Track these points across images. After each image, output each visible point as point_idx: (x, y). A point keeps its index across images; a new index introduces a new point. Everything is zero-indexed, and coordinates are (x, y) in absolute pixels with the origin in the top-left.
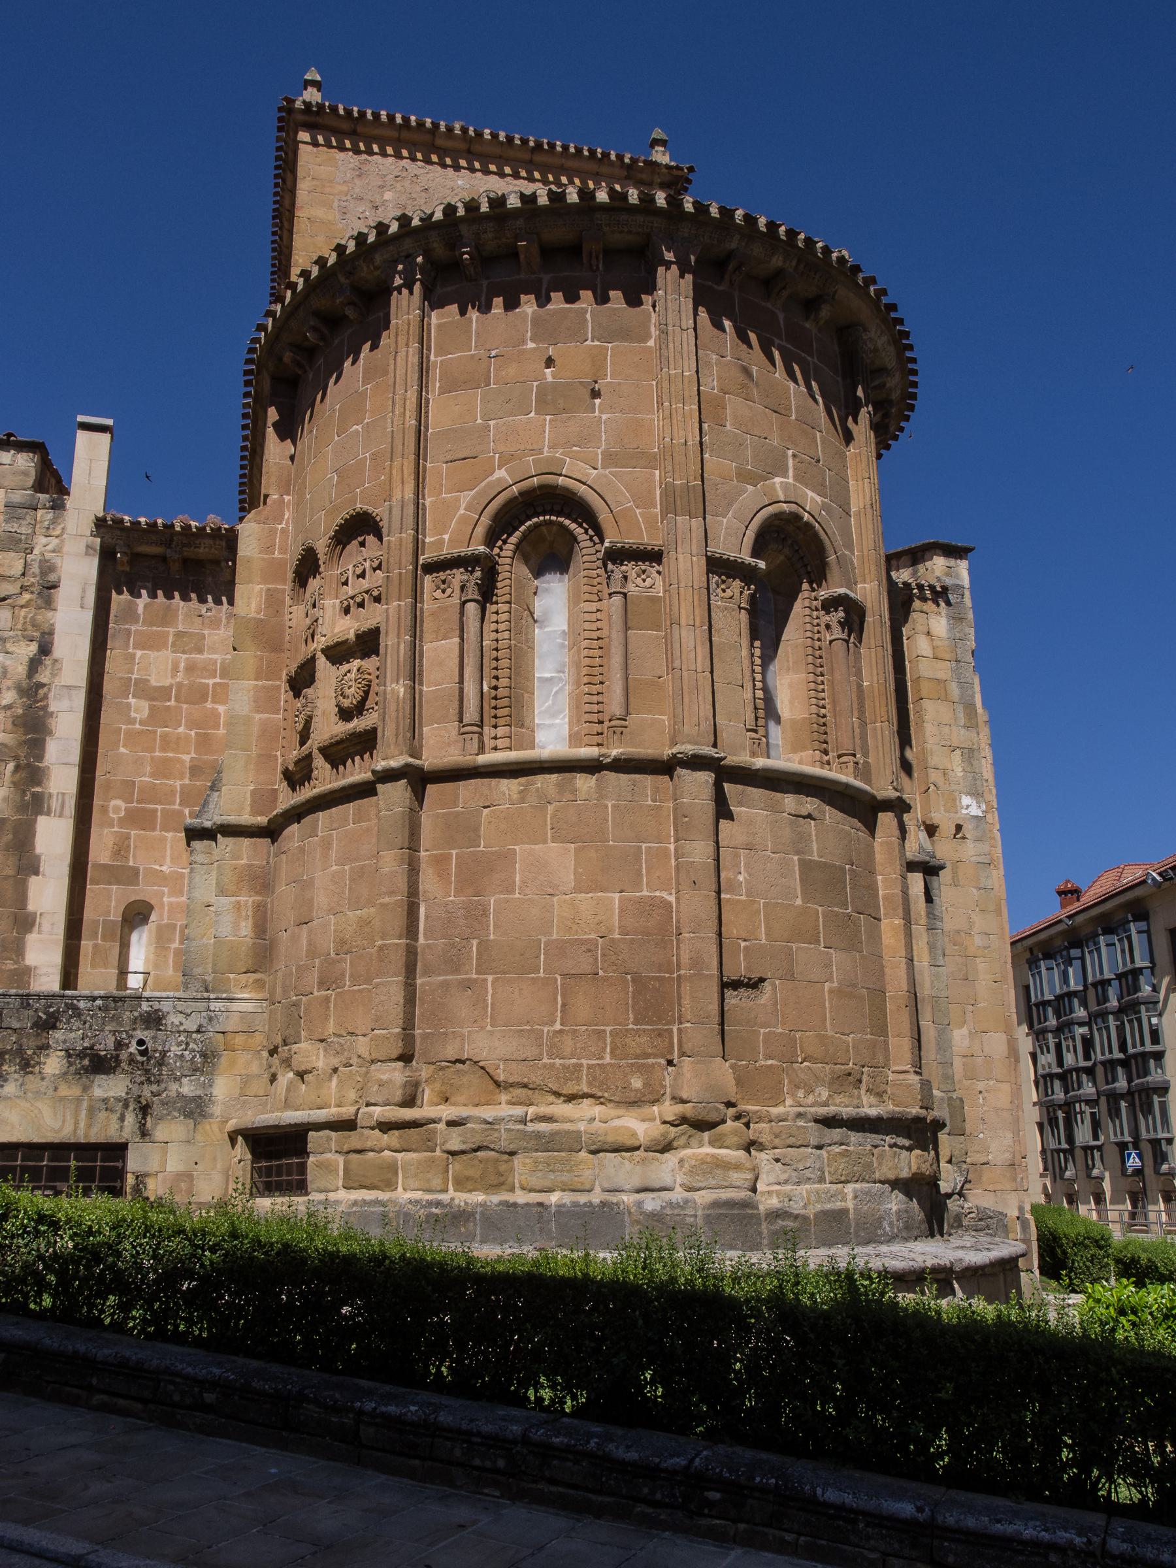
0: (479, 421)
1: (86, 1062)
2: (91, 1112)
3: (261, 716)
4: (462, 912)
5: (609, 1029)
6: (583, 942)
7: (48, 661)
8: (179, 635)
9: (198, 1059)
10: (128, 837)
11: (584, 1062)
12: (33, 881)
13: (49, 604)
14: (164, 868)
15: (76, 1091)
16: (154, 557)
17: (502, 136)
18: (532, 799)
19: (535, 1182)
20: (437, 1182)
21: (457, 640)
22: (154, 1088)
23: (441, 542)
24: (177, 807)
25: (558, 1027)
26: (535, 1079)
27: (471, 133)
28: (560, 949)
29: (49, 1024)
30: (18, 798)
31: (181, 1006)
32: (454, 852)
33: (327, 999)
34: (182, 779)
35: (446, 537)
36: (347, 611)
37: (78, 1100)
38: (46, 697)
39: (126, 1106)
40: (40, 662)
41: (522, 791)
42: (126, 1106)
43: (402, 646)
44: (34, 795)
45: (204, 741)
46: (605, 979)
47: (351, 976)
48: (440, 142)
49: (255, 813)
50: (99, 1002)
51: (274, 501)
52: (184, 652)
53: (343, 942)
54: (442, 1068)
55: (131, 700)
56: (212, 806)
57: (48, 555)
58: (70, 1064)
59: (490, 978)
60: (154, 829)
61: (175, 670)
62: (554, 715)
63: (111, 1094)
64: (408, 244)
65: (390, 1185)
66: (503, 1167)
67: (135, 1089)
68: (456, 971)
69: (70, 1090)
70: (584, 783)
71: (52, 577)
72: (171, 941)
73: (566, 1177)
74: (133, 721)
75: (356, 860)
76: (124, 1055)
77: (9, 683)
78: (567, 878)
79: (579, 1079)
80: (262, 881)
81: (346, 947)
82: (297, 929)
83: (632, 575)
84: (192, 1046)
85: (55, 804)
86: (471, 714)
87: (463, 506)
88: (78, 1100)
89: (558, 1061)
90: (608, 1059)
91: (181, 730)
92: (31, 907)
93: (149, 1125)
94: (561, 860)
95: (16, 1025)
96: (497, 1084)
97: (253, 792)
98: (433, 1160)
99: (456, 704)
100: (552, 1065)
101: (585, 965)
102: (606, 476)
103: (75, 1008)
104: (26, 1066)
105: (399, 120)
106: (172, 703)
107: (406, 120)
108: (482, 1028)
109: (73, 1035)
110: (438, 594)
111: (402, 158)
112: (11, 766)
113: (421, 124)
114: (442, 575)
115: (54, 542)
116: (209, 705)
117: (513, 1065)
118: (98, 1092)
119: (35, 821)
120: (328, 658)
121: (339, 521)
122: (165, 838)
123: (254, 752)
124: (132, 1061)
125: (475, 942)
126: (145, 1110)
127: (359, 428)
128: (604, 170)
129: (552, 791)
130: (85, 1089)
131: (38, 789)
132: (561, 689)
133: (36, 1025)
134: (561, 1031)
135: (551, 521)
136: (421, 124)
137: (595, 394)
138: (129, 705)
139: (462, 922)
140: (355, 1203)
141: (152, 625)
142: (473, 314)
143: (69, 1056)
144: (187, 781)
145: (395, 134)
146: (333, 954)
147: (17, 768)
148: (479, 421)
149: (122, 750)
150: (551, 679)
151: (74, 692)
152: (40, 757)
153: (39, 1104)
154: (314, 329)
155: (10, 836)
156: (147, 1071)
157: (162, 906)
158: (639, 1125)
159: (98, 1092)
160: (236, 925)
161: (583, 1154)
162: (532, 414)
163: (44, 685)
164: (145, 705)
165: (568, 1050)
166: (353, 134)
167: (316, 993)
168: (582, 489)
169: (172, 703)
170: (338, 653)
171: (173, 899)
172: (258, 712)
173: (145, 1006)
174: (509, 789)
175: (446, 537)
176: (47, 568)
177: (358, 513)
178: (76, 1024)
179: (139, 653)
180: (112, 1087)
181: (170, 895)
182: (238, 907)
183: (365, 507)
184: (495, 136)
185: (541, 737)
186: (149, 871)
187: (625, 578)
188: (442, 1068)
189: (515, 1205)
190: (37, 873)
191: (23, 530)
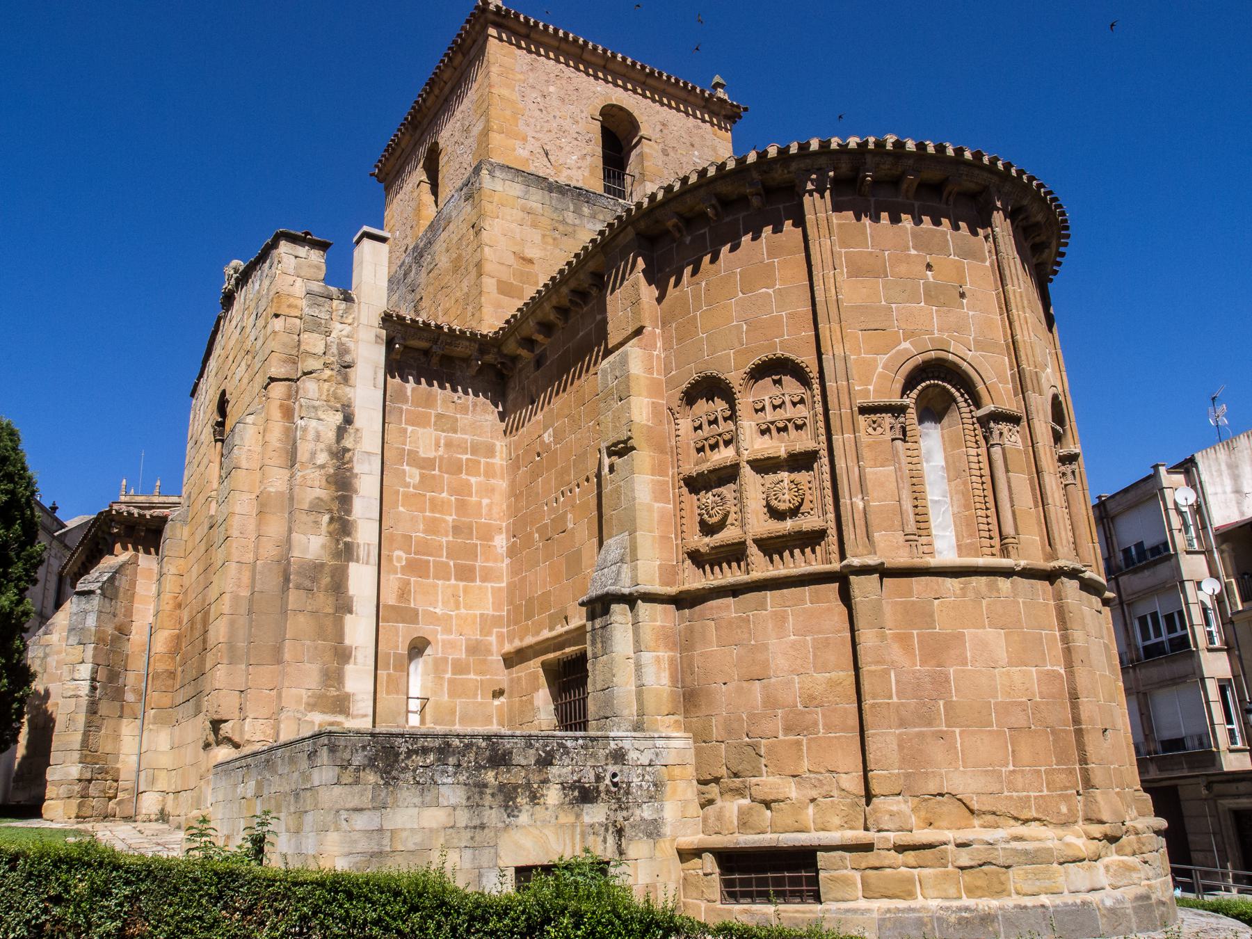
1: (576, 793)
2: (583, 835)
4: (927, 679)
5: (1043, 769)
6: (1021, 703)
7: (351, 429)
8: (439, 416)
9: (652, 789)
10: (408, 583)
11: (1032, 794)
12: (348, 618)
13: (346, 380)
14: (437, 610)
15: (571, 819)
16: (417, 350)
17: (629, 61)
18: (971, 595)
19: (1027, 888)
20: (952, 892)
22: (625, 813)
23: (868, 391)
24: (444, 559)
25: (1011, 768)
26: (1001, 808)
27: (609, 54)
28: (1005, 708)
29: (546, 761)
30: (333, 546)
31: (637, 744)
32: (915, 632)
33: (799, 743)
34: (447, 536)
35: (871, 388)
36: (763, 432)
37: (573, 826)
38: (351, 461)
39: (607, 830)
40: (345, 430)
42: (607, 830)
44: (346, 544)
45: (462, 506)
46: (1036, 731)
47: (825, 725)
48: (586, 56)
49: (664, 584)
50: (580, 742)
52: (443, 431)
53: (812, 698)
54: (925, 800)
55: (406, 468)
57: (344, 340)
58: (566, 795)
59: (957, 730)
60: (428, 577)
61: (438, 446)
62: (944, 529)
63: (595, 820)
64: (823, 161)
65: (910, 895)
66: (1003, 878)
67: (612, 818)
68: (930, 724)
69: (567, 818)
70: (1004, 584)
71: (348, 358)
72: (445, 671)
73: (1047, 883)
74: (408, 485)
75: (819, 632)
76: (602, 787)
77: (322, 446)
78: (1002, 654)
79: (1030, 807)
80: (685, 644)
81: (816, 702)
82: (745, 684)
83: (1005, 431)
84: (647, 777)
85: (362, 553)
88: (573, 826)
89: (1015, 794)
90: (1045, 792)
91: (444, 495)
92: (348, 642)
93: (623, 845)
94: (996, 640)
95: (524, 762)
96: (972, 812)
98: (947, 874)
100: (1011, 797)
101: (1019, 719)
103: (565, 747)
104: (534, 798)
105: (561, 33)
106: (436, 472)
107: (566, 35)
108: (957, 769)
109: (565, 770)
110: (870, 430)
111: (559, 62)
112: (326, 518)
113: (575, 41)
114: (874, 417)
115: (348, 329)
116: (464, 476)
117: (984, 798)
118: (587, 819)
119: (347, 566)
120: (752, 468)
121: (756, 361)
122: (437, 585)
123: (657, 534)
124: (608, 792)
125: (941, 703)
126: (620, 832)
127: (771, 291)
128: (691, 99)
129: (984, 590)
130: (578, 816)
131: (348, 539)
133: (537, 762)
134: (1014, 771)
135: (938, 385)
136: (575, 41)
137: (962, 295)
138: (404, 471)
139: (929, 686)
140: (889, 911)
141: (419, 406)
142: (866, 221)
143: (564, 788)
144: (450, 538)
145: (556, 43)
146: (800, 707)
147: (332, 520)
149: (401, 509)
151: (373, 458)
152: (349, 512)
153: (546, 831)
154: (713, 207)
155: (328, 579)
156: (619, 800)
157: (437, 642)
158: (1077, 840)
159: (587, 819)
160: (658, 678)
161: (1055, 865)
163: (349, 450)
165: (1020, 786)
166: (527, 37)
167: (781, 737)
168: (965, 365)
169: (436, 472)
171: (445, 637)
173: (613, 745)
175: (871, 388)
176: (343, 351)
177: (778, 358)
178: (567, 761)
179: (410, 428)
180: (596, 814)
181: (443, 633)
182: (658, 660)
183: (787, 355)
184: (624, 59)
185: (938, 544)
186: (426, 612)
187: (1001, 434)
188: (925, 800)
189: (1025, 907)
190: (351, 612)
191: (322, 315)
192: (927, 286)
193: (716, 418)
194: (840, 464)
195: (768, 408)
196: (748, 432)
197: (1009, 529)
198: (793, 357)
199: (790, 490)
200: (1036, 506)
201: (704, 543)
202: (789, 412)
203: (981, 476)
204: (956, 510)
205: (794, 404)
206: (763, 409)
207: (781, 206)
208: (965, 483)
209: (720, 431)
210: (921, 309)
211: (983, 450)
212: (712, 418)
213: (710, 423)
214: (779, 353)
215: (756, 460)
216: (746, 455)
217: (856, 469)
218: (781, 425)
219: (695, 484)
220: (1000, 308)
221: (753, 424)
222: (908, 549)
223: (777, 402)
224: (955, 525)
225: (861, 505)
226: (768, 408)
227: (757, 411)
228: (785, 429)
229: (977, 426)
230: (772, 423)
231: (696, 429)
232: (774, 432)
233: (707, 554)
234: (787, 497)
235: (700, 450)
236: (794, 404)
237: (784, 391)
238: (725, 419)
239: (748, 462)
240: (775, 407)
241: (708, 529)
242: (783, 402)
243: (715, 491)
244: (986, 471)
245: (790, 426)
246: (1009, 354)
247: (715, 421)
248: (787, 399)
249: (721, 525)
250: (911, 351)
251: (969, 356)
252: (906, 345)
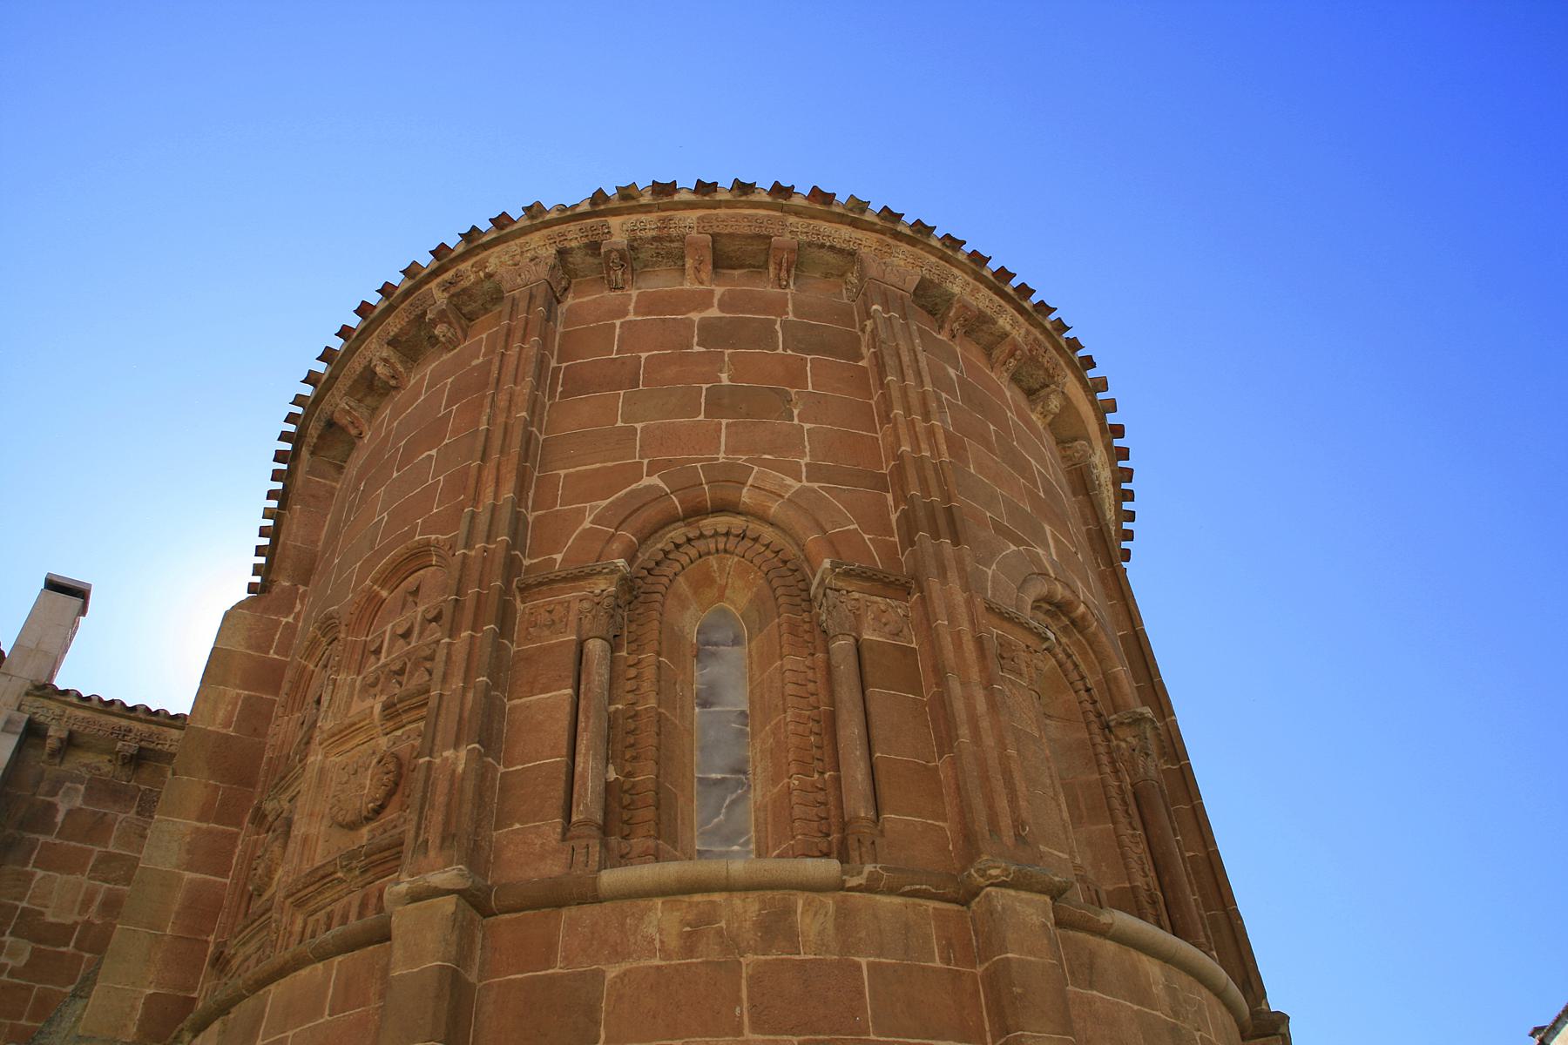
0: (619, 424)
8: (108, 858)
21: (569, 691)
41: (689, 934)
43: (470, 696)
51: (283, 589)
52: (106, 881)
61: (86, 905)
62: (729, 840)
86: (588, 804)
99: (561, 786)
102: (814, 491)
150: (723, 779)
154: (386, 360)
162: (702, 417)
164: (27, 947)
172: (190, 867)
174: (660, 930)
175: (559, 557)
179: (40, 873)
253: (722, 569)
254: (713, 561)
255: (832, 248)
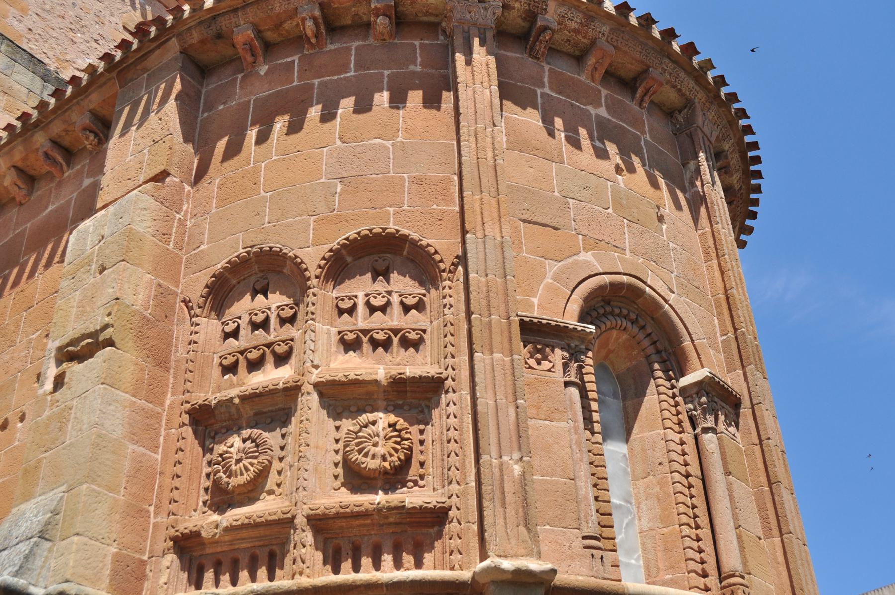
0: (556, 193)
3: (135, 447)
35: (535, 301)
56: (39, 562)
87: (550, 274)
97: (118, 559)
110: (532, 362)
120: (321, 395)
121: (352, 234)
127: (388, 144)
132: (631, 522)
148: (556, 193)
170: (342, 398)
183: (404, 231)
192: (616, 192)
193: (267, 320)
194: (486, 402)
195: (361, 309)
196: (322, 341)
197: (732, 560)
198: (415, 236)
199: (387, 439)
200: (768, 535)
201: (209, 522)
202: (395, 319)
203: (687, 476)
204: (645, 524)
205: (406, 309)
206: (351, 311)
207: (417, 43)
208: (661, 483)
209: (271, 338)
210: (608, 216)
211: (688, 437)
212: (260, 318)
213: (255, 326)
214: (392, 227)
215: (333, 383)
216: (315, 376)
217: (512, 411)
218: (381, 336)
219: (208, 423)
220: (706, 253)
221: (334, 331)
222: (588, 560)
223: (378, 302)
224: (645, 549)
225: (517, 469)
226: (361, 309)
227: (341, 312)
228: (386, 345)
229: (679, 399)
230: (365, 332)
231: (227, 336)
232: (367, 347)
233: (214, 542)
234: (380, 450)
235: (230, 369)
236: (406, 309)
237: (392, 287)
238: (283, 321)
239: (316, 385)
240: (372, 309)
241: (222, 498)
242: (389, 303)
243: (246, 433)
244: (694, 469)
245: (396, 340)
246: (720, 314)
247: (264, 325)
248: (395, 299)
249: (251, 492)
250: (596, 265)
251: (672, 297)
252: (586, 256)
253: (617, 339)
254: (614, 333)
255: (680, 90)
